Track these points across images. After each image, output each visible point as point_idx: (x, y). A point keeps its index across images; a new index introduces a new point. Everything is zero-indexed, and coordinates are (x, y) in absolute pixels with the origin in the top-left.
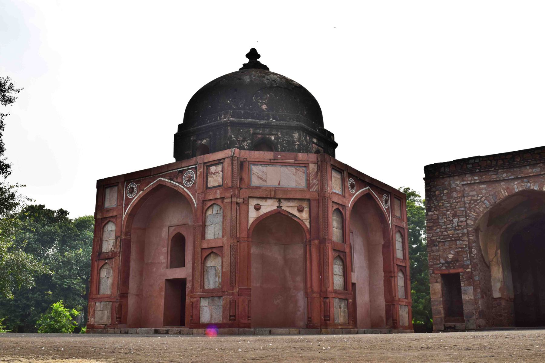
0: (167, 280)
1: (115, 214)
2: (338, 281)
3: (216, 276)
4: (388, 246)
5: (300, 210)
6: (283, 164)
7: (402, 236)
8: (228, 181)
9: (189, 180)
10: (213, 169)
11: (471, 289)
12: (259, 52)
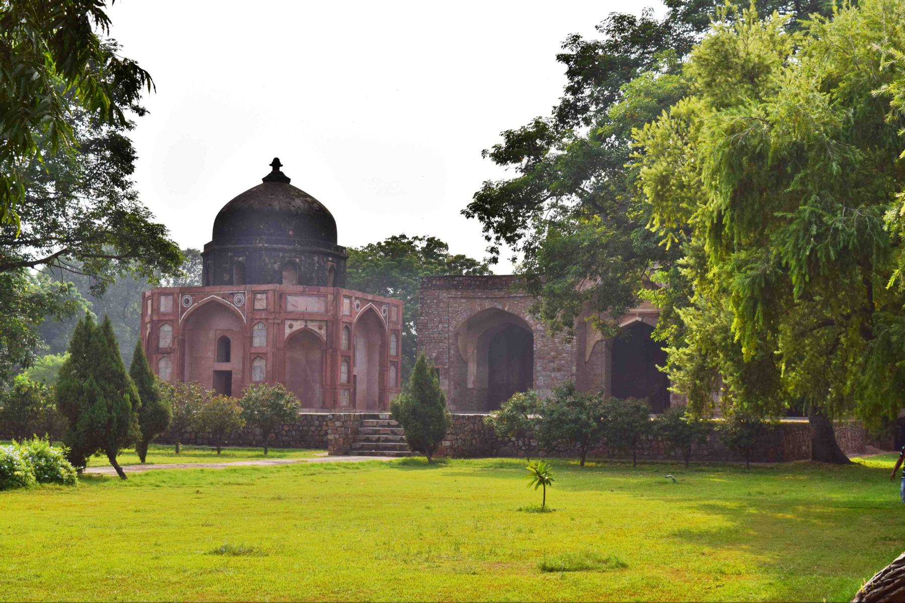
0: (218, 373)
1: (171, 318)
2: (343, 377)
3: (261, 372)
4: (384, 346)
5: (320, 328)
6: (309, 295)
7: (397, 337)
8: (271, 307)
9: (240, 301)
10: (259, 296)
11: (446, 382)
12: (282, 162)
